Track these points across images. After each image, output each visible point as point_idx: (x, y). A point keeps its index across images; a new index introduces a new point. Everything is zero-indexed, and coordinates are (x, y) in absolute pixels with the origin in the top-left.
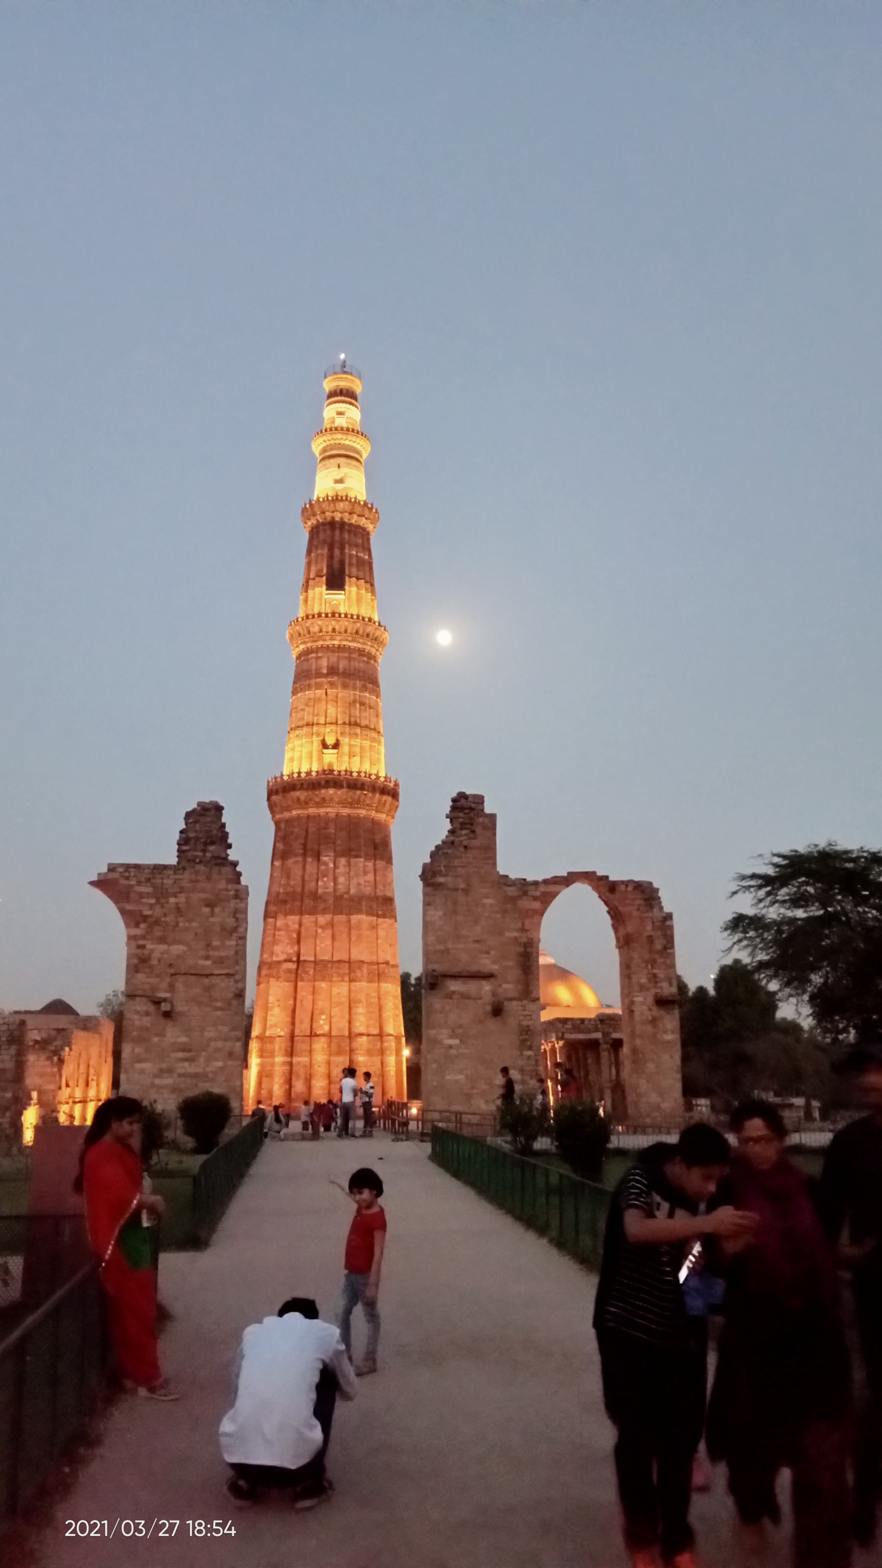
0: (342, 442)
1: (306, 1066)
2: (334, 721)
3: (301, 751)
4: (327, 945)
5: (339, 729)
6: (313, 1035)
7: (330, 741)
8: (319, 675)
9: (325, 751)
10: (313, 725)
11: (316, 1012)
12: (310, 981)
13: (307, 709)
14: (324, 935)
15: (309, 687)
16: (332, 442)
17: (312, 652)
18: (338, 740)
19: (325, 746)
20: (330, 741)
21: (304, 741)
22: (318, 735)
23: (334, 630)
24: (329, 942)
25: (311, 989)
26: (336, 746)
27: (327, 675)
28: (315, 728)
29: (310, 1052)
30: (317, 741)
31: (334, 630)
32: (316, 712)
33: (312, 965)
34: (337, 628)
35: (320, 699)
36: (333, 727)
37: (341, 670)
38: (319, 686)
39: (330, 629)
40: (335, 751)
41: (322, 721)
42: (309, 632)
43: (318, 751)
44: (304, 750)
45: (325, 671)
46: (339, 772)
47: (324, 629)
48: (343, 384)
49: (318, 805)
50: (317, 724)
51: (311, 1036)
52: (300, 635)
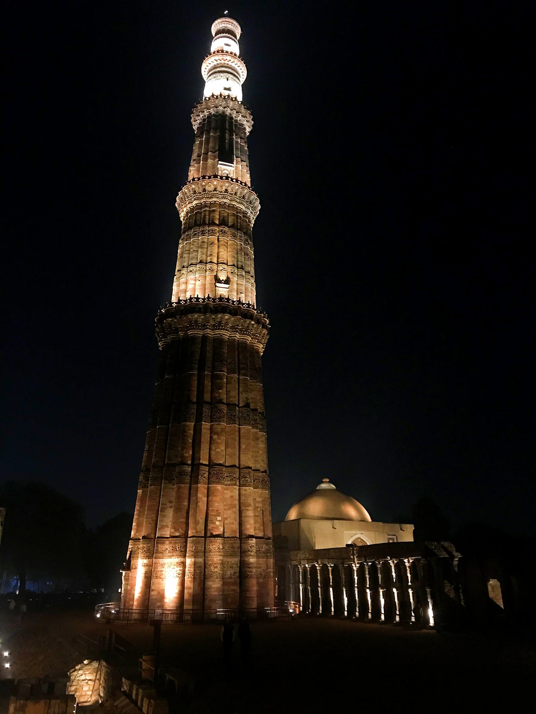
0: (230, 63)
1: (200, 567)
2: (225, 262)
3: (195, 284)
4: (221, 450)
5: (229, 269)
6: (208, 535)
7: (223, 277)
8: (213, 224)
9: (218, 284)
10: (206, 263)
11: (211, 513)
12: (205, 483)
13: (200, 250)
14: (220, 441)
15: (203, 233)
16: (222, 62)
17: (206, 206)
18: (228, 278)
19: (217, 280)
20: (223, 277)
21: (197, 276)
22: (211, 270)
23: (226, 191)
24: (223, 448)
25: (206, 491)
26: (227, 281)
27: (219, 225)
28: (209, 266)
29: (205, 552)
30: (209, 277)
31: (226, 191)
32: (209, 253)
33: (207, 468)
34: (229, 190)
35: (212, 243)
36: (225, 266)
37: (230, 224)
38: (213, 233)
39: (224, 189)
40: (227, 286)
41: (215, 260)
42: (204, 190)
43: (211, 284)
44: (198, 283)
45: (217, 222)
46: (233, 302)
47: (219, 189)
48: (230, 26)
49: (214, 327)
50: (211, 262)
51: (205, 537)
52: (195, 192)
